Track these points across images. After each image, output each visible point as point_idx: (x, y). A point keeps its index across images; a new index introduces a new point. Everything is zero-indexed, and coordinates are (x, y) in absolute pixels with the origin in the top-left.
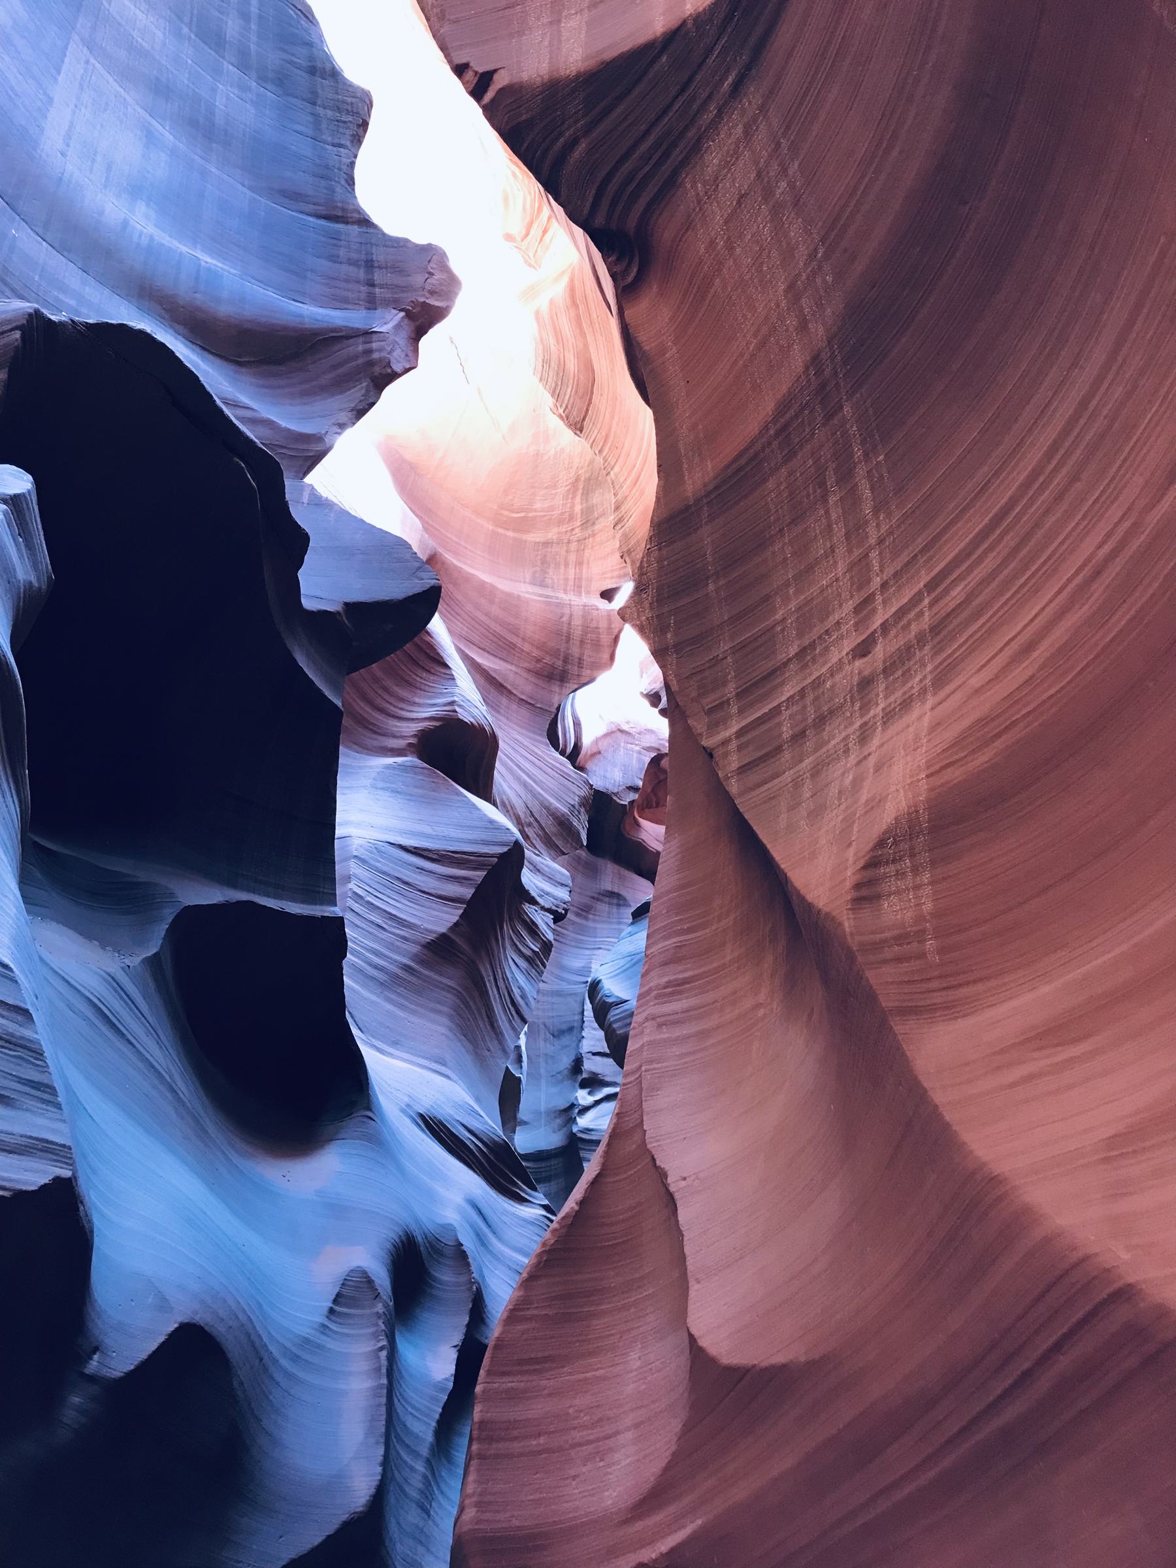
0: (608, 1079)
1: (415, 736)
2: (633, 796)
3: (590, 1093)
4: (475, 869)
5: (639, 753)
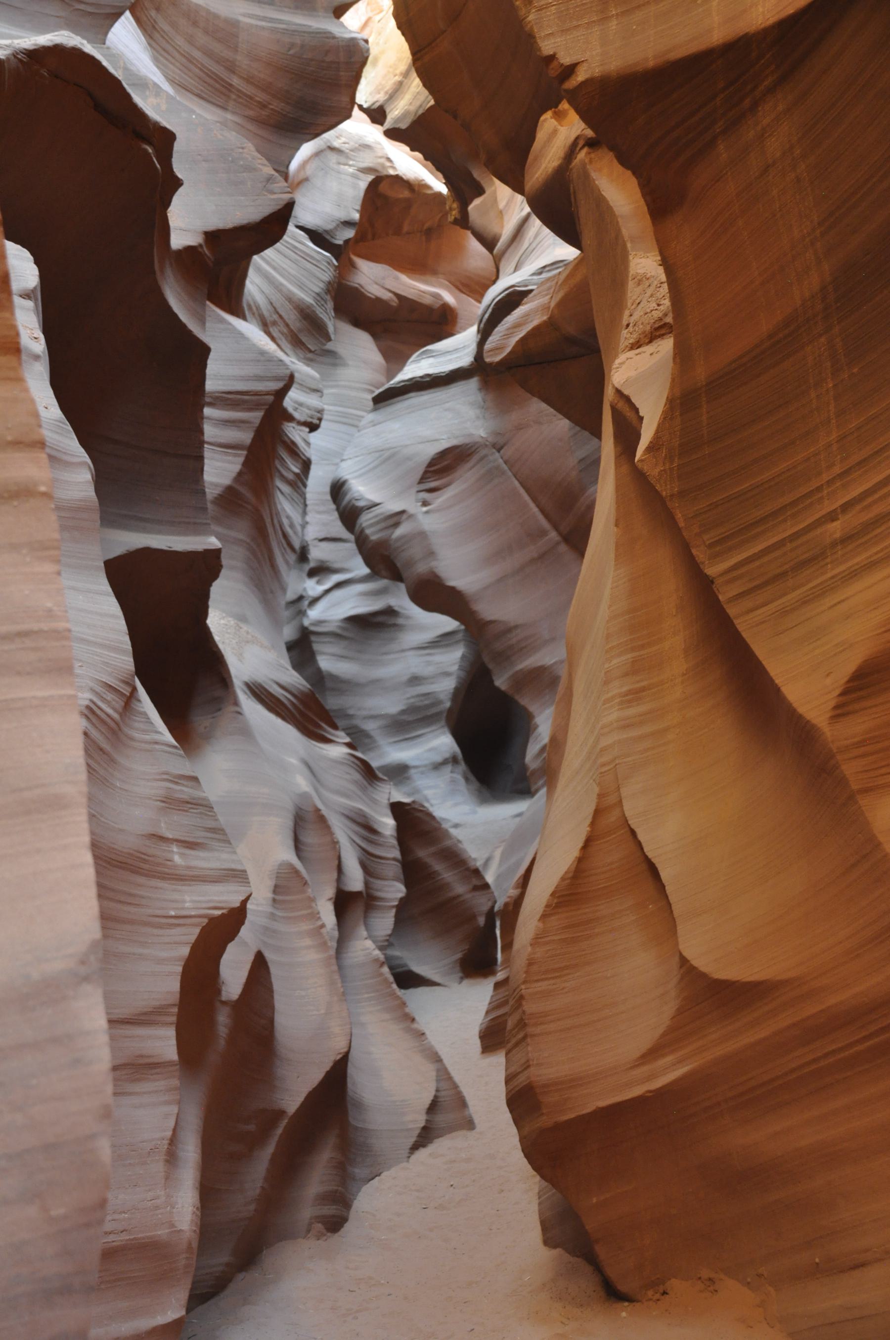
0: (336, 566)
3: (318, 582)
4: (250, 410)
5: (353, 176)
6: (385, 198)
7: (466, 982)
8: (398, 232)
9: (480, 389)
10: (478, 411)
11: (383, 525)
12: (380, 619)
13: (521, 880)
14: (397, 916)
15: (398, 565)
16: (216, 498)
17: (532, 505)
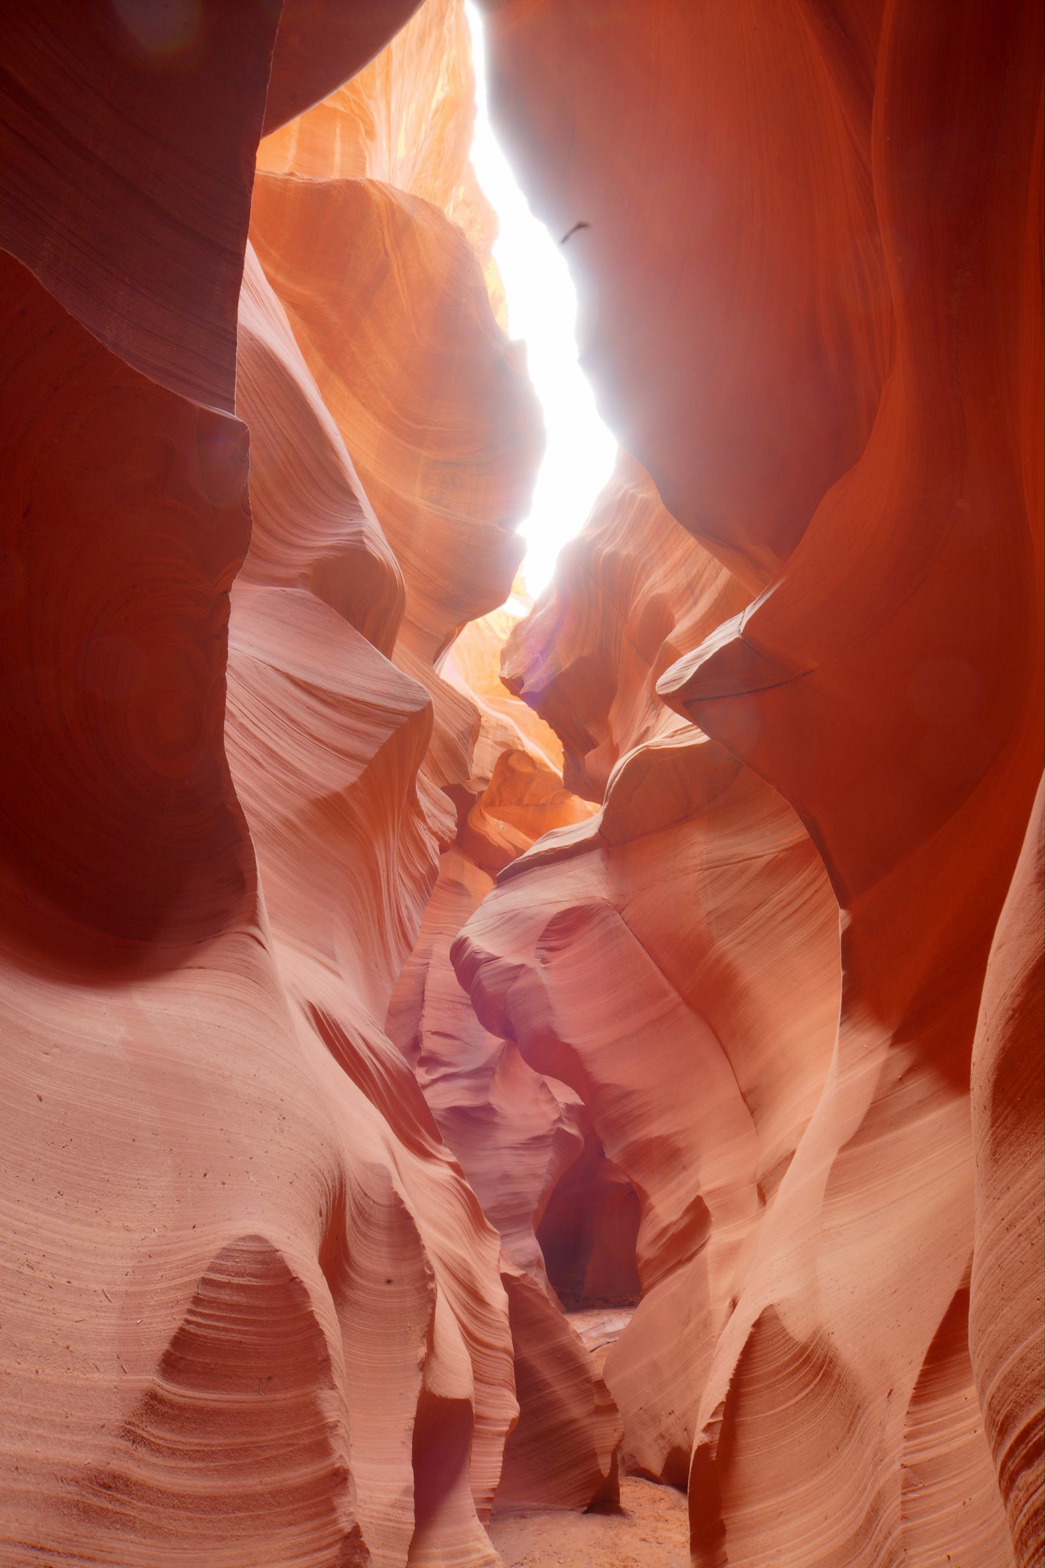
0: (445, 1059)
1: (309, 565)
2: (484, 788)
3: (427, 1072)
4: (379, 725)
6: (512, 771)
8: (519, 803)
9: (602, 859)
16: (318, 799)
17: (653, 965)
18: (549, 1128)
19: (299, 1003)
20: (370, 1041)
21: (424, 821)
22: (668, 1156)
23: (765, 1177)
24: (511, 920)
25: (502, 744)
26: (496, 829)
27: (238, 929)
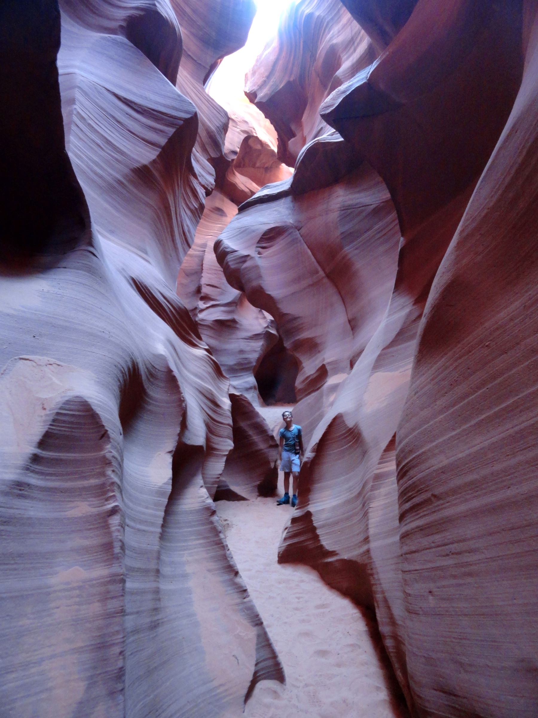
0: (212, 297)
1: (124, 20)
2: (235, 157)
3: (204, 303)
5: (238, 133)
6: (251, 148)
7: (259, 499)
8: (254, 166)
9: (292, 201)
10: (290, 211)
11: (238, 261)
12: (229, 323)
13: (316, 447)
14: (227, 462)
15: (243, 281)
16: (134, 168)
17: (313, 258)
18: (262, 330)
19: (125, 277)
20: (164, 294)
21: (197, 178)
22: (312, 346)
23: (354, 357)
24: (244, 232)
25: (244, 132)
26: (242, 181)
27: (81, 248)
